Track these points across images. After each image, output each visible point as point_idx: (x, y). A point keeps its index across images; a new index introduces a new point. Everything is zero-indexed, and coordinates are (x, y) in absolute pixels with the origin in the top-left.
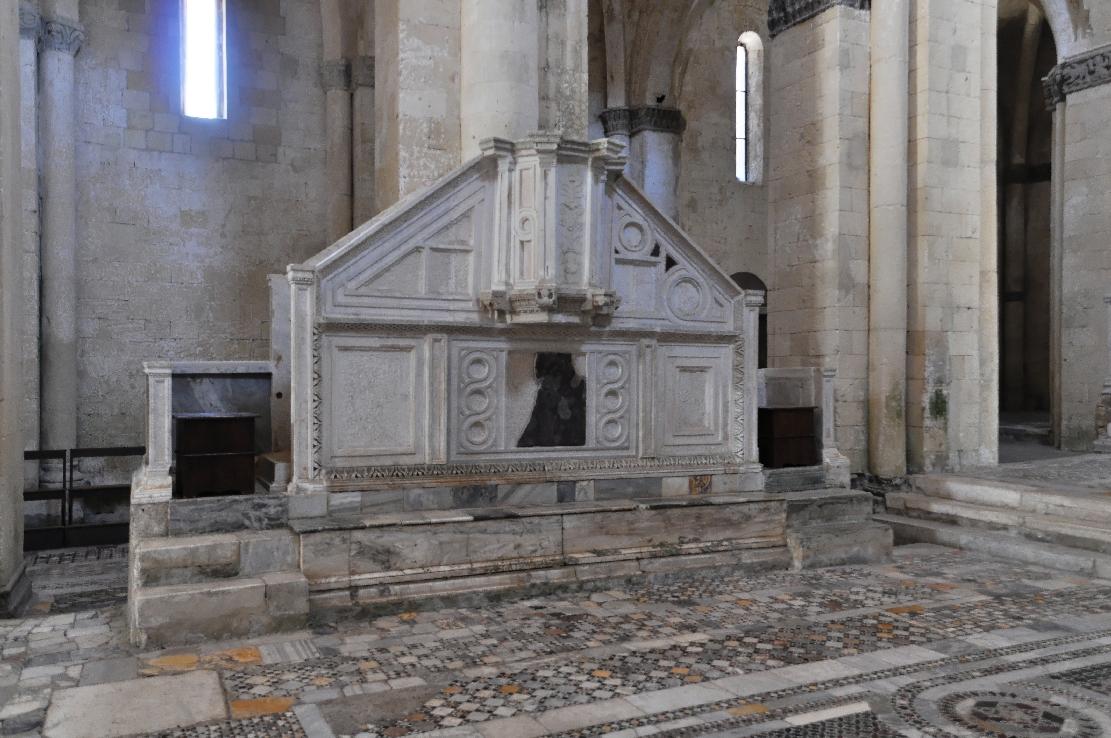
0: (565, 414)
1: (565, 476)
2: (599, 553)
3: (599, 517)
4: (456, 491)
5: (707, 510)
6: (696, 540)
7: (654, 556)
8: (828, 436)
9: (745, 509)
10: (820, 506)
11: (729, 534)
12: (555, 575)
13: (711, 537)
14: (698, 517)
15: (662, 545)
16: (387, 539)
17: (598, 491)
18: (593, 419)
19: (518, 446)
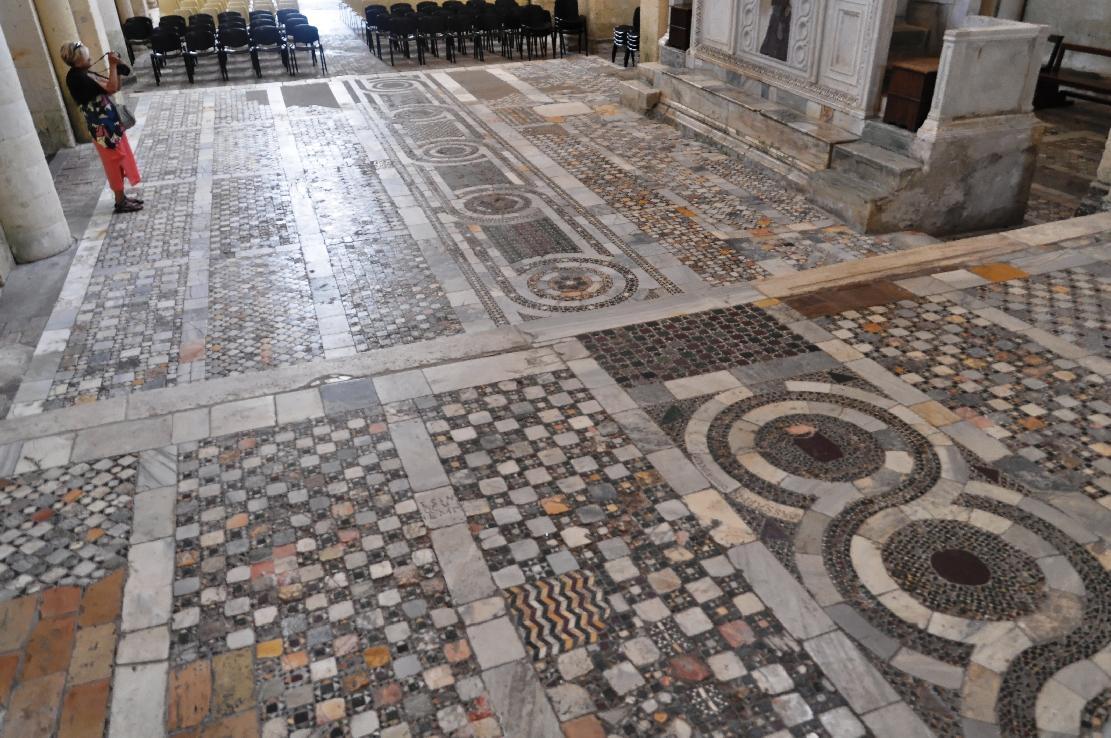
0: (780, 37)
1: (765, 79)
2: (738, 133)
3: (741, 109)
4: (729, 72)
5: (786, 130)
6: (778, 149)
7: (758, 149)
8: (936, 107)
9: (806, 138)
10: (858, 162)
11: (793, 153)
12: (718, 136)
13: (786, 151)
14: (782, 132)
15: (763, 143)
16: (681, 87)
17: (778, 96)
18: (792, 43)
19: (762, 52)
